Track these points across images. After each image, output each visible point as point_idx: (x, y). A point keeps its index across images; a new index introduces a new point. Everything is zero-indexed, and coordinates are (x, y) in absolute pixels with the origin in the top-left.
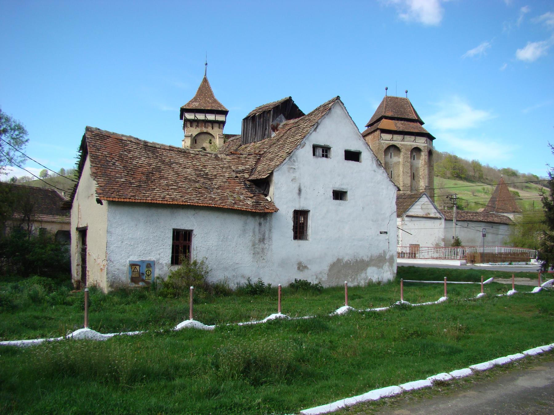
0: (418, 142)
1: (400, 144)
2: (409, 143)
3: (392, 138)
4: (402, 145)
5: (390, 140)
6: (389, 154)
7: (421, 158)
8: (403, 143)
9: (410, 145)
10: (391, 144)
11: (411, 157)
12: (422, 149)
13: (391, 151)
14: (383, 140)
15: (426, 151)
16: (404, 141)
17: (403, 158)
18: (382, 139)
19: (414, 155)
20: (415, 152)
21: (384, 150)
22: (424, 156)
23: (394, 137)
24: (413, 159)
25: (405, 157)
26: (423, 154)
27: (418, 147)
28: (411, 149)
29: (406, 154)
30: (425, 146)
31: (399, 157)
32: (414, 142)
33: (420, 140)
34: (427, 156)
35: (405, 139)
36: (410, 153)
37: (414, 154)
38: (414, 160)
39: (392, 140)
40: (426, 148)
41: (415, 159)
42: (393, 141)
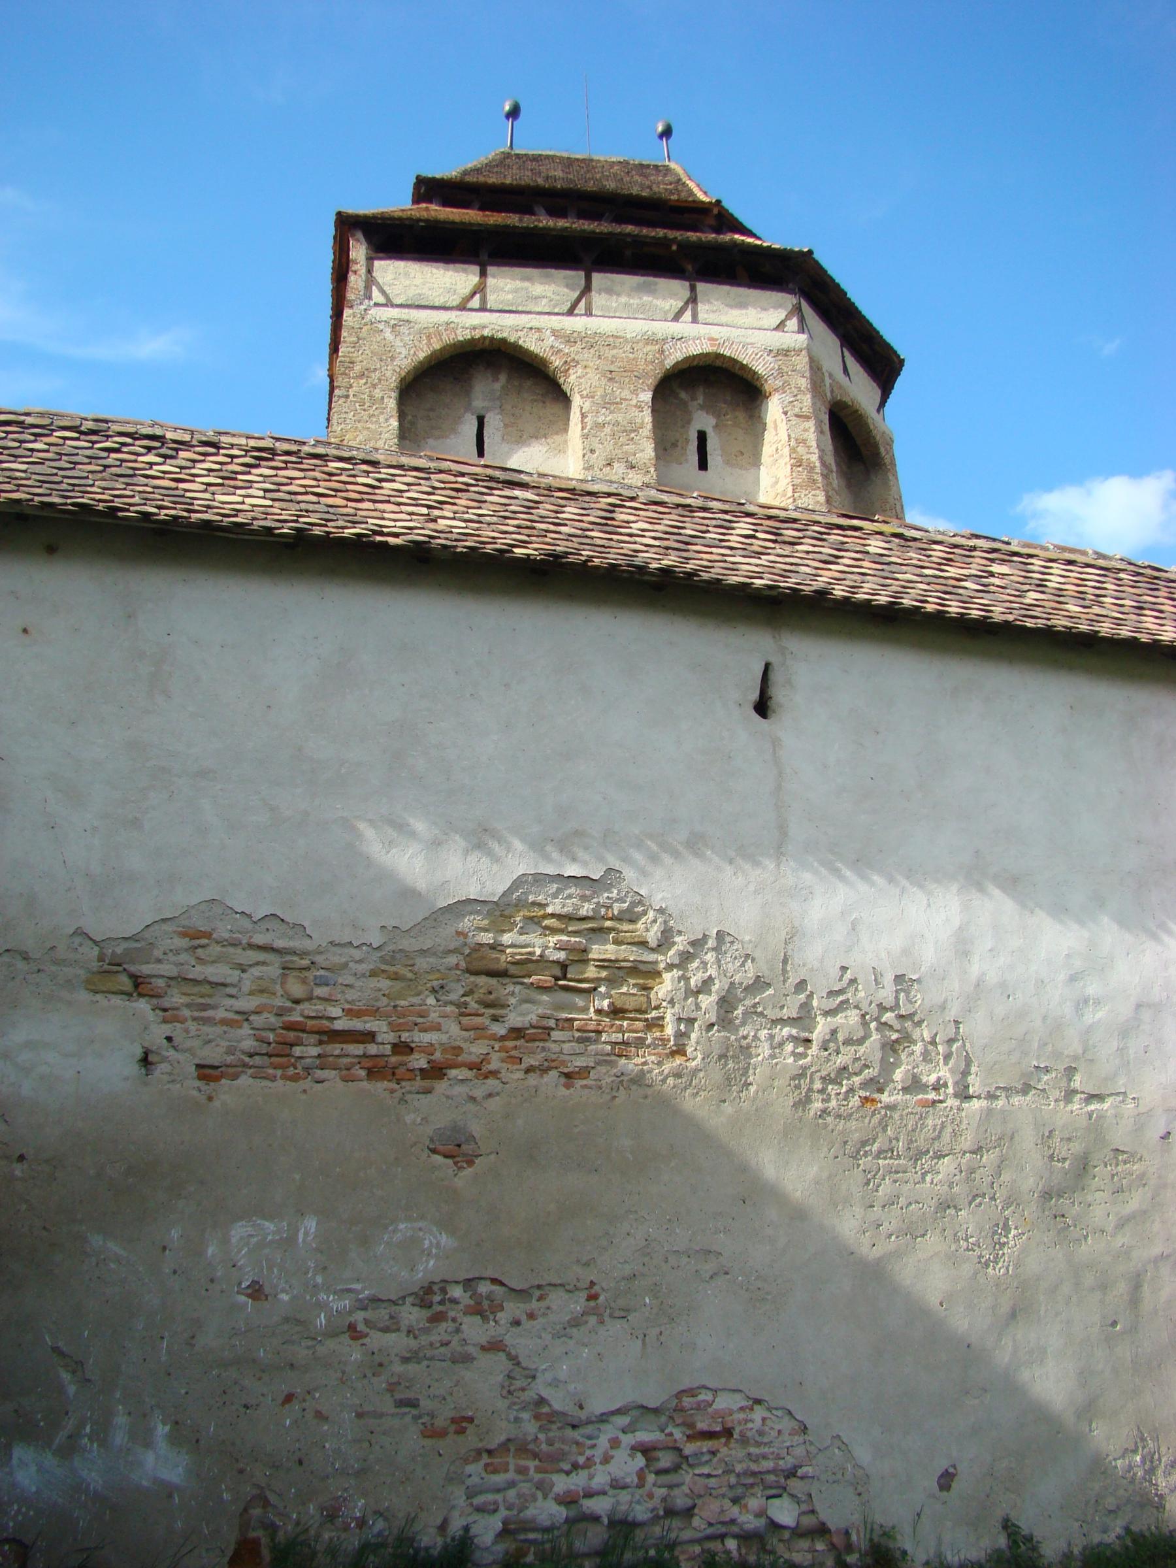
0: (723, 319)
1: (555, 333)
2: (635, 327)
3: (480, 289)
4: (570, 339)
5: (462, 307)
6: (458, 420)
7: (767, 450)
8: (577, 323)
9: (650, 340)
10: (463, 335)
11: (665, 447)
12: (761, 366)
13: (479, 403)
14: (389, 304)
15: (804, 383)
16: (589, 313)
17: (585, 437)
18: (377, 296)
19: (702, 437)
20: (707, 408)
21: (393, 381)
22: (783, 428)
23: (491, 281)
24: (694, 458)
25: (601, 426)
26: (774, 409)
27: (727, 353)
28: (659, 373)
29: (609, 404)
30: (785, 352)
31: (561, 450)
32: (688, 315)
33: (742, 305)
34: (811, 425)
35: (598, 299)
36: (647, 396)
37: (703, 420)
38: (703, 465)
39: (475, 302)
40: (802, 362)
41: (713, 459)
42: (483, 309)
